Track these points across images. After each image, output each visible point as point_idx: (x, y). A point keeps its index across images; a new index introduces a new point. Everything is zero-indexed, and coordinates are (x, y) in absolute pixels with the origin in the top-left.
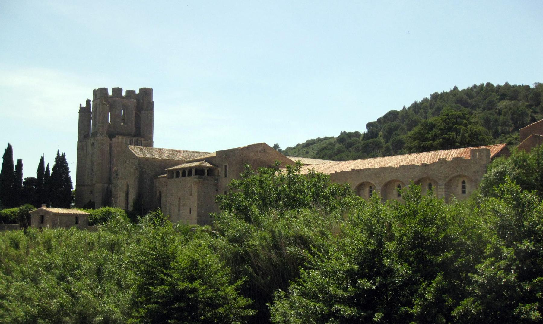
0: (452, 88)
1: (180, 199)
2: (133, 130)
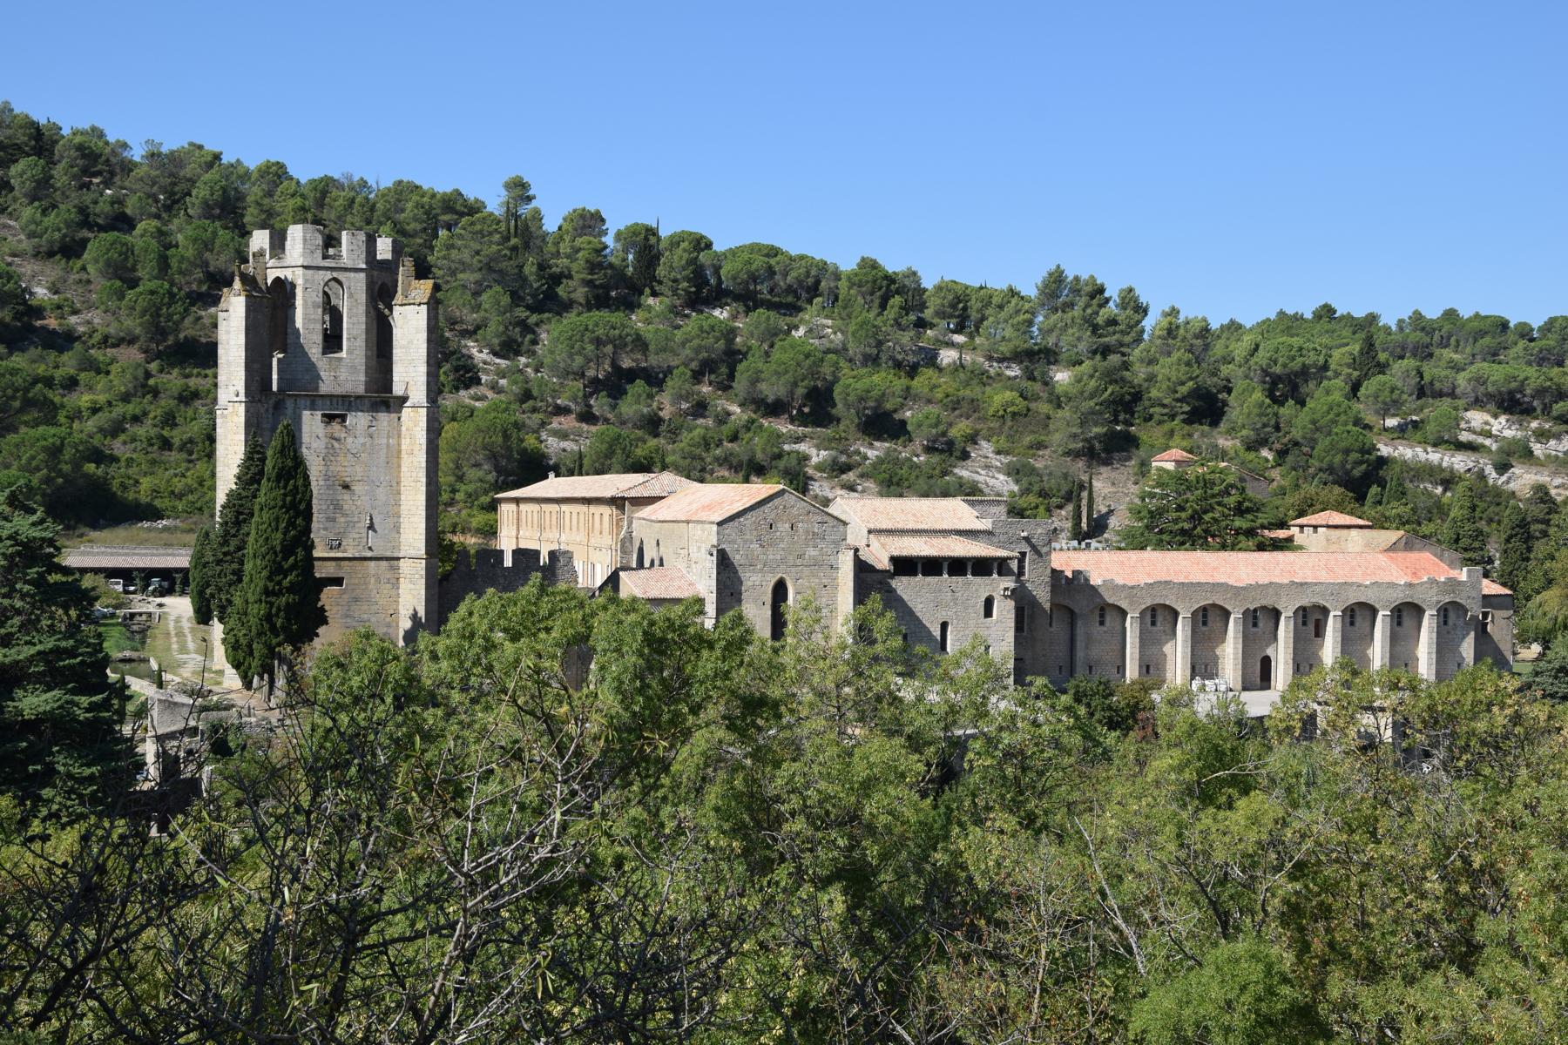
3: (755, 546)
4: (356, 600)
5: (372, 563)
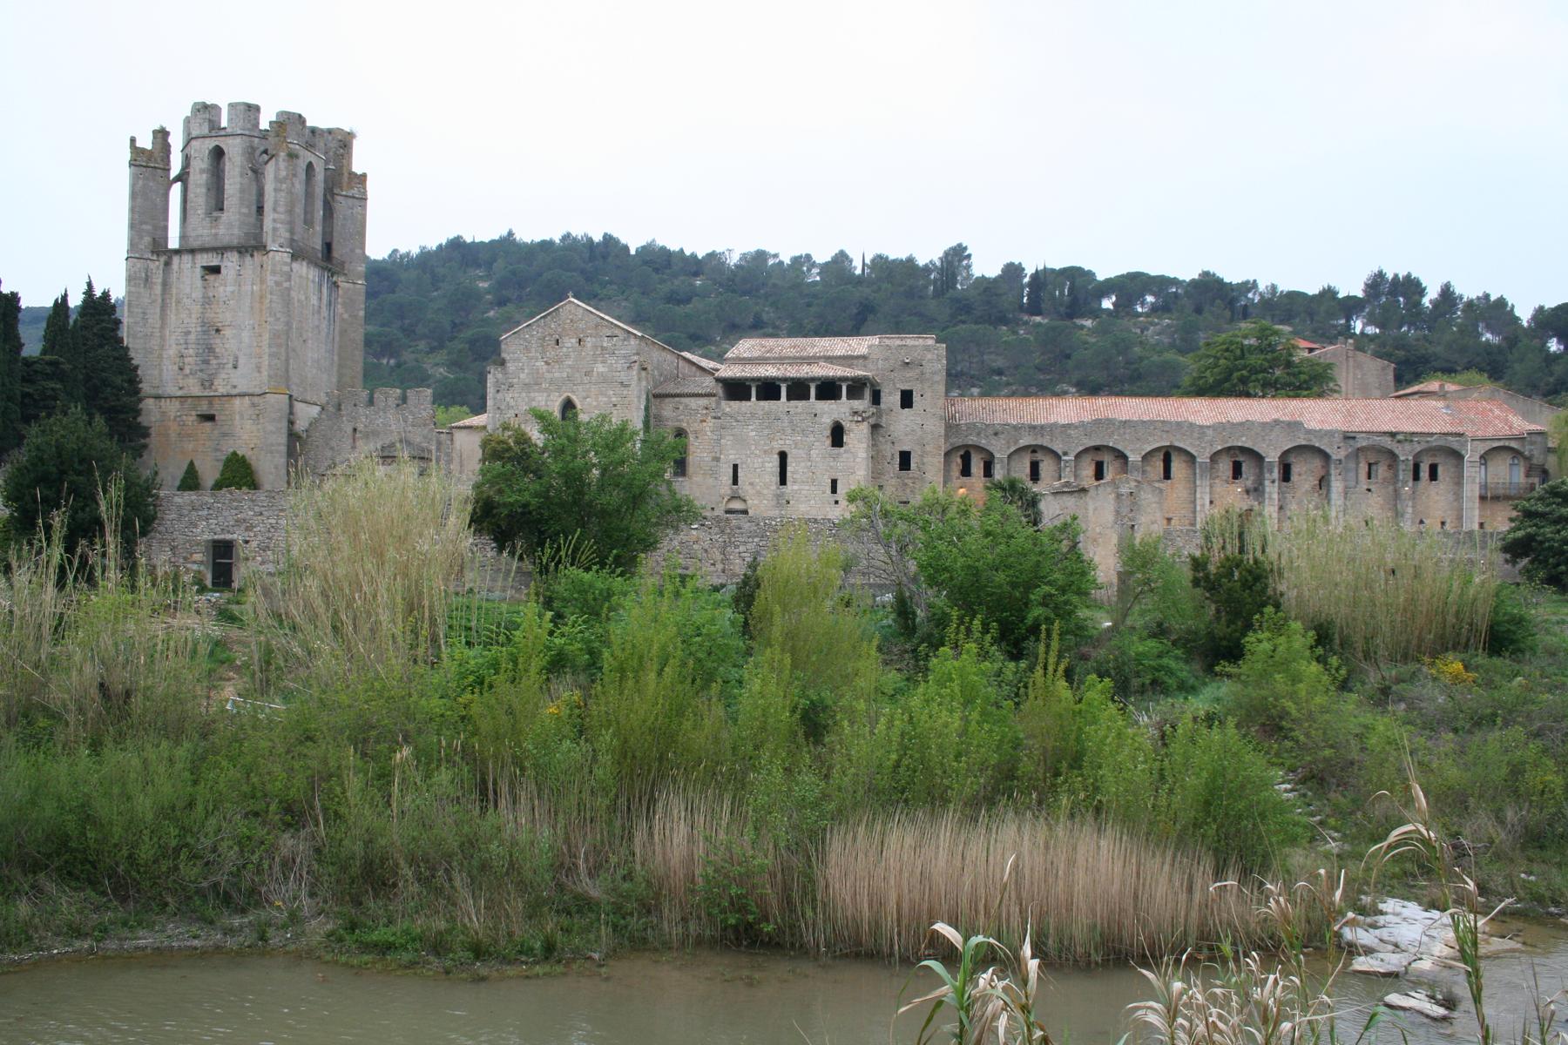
0: (505, 233)
1: (783, 456)
2: (318, 244)
3: (540, 364)
4: (225, 435)
5: (237, 401)
